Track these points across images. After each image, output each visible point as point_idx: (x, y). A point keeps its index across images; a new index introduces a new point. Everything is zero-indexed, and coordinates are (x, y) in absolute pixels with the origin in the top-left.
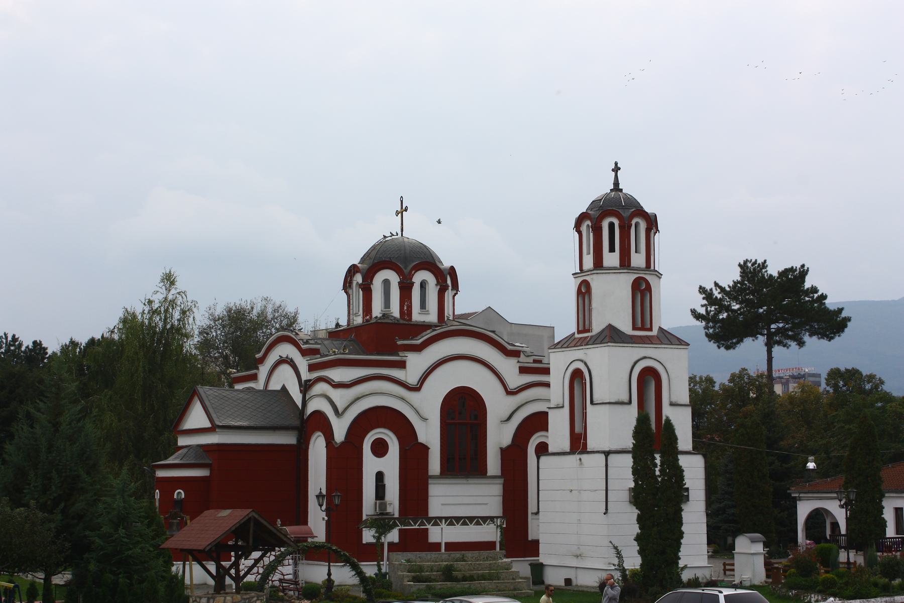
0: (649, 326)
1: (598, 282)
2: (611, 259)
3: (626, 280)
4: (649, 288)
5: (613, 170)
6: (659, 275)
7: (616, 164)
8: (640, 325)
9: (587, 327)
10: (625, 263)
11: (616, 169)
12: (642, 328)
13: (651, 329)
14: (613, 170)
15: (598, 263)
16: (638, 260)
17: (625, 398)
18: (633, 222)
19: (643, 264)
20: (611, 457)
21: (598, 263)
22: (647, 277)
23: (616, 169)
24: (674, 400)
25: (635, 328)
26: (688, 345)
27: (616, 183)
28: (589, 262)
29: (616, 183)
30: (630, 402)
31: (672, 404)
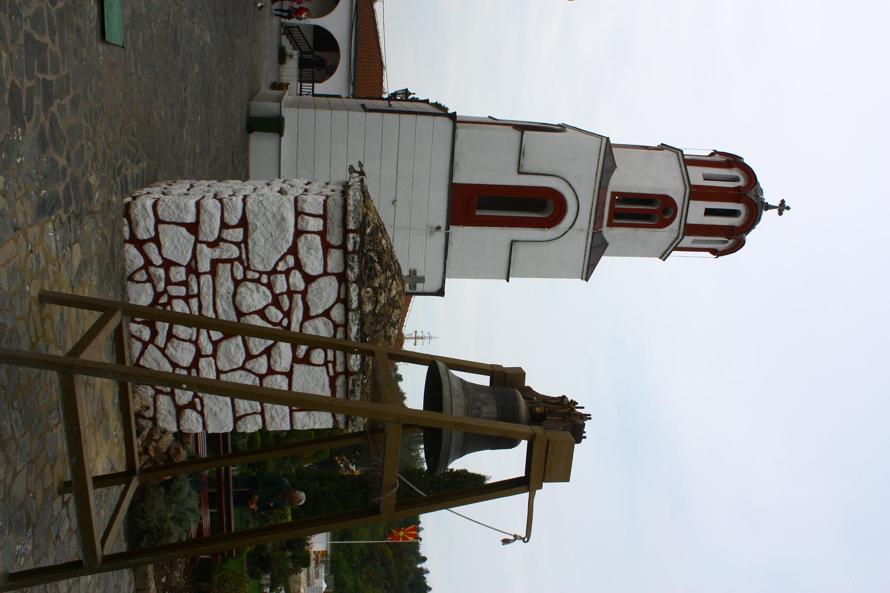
0: (615, 221)
2: (697, 176)
3: (674, 189)
4: (664, 224)
6: (664, 256)
7: (788, 208)
13: (610, 224)
17: (527, 166)
18: (740, 207)
19: (691, 220)
22: (675, 224)
24: (519, 249)
26: (587, 280)
27: (768, 207)
29: (768, 207)
30: (520, 173)
31: (513, 242)
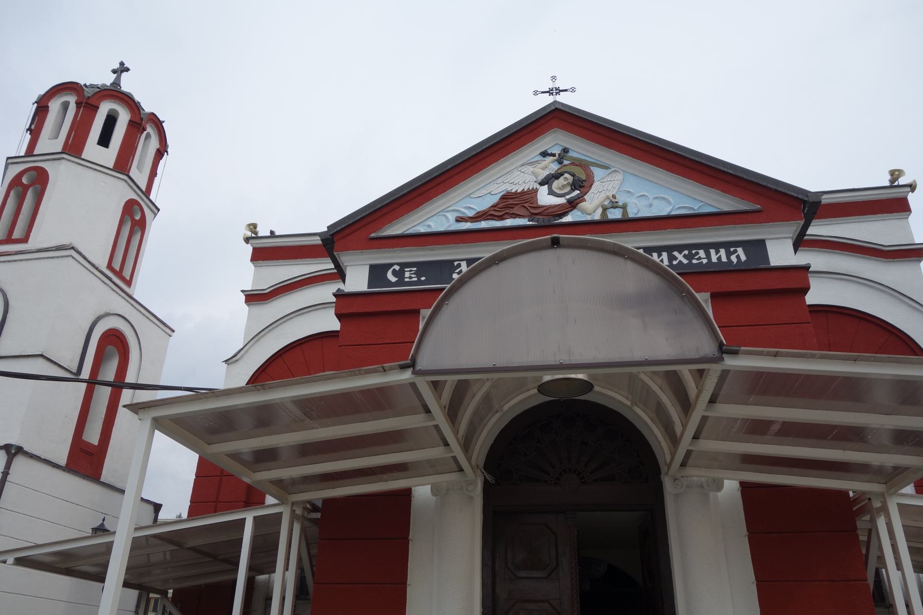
1: (62, 174)
5: (114, 72)
7: (122, 64)
8: (117, 268)
9: (16, 235)
10: (122, 165)
11: (122, 69)
12: (119, 274)
13: (129, 283)
14: (114, 72)
15: (74, 147)
16: (140, 176)
20: (20, 462)
21: (74, 147)
23: (122, 69)
25: (110, 266)
27: (117, 83)
28: (49, 143)
29: (117, 83)
